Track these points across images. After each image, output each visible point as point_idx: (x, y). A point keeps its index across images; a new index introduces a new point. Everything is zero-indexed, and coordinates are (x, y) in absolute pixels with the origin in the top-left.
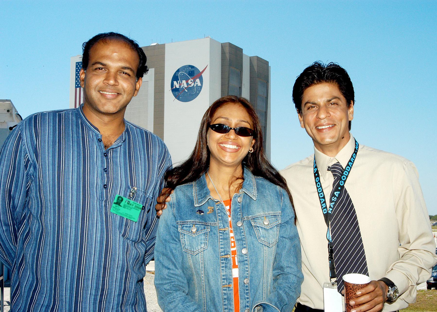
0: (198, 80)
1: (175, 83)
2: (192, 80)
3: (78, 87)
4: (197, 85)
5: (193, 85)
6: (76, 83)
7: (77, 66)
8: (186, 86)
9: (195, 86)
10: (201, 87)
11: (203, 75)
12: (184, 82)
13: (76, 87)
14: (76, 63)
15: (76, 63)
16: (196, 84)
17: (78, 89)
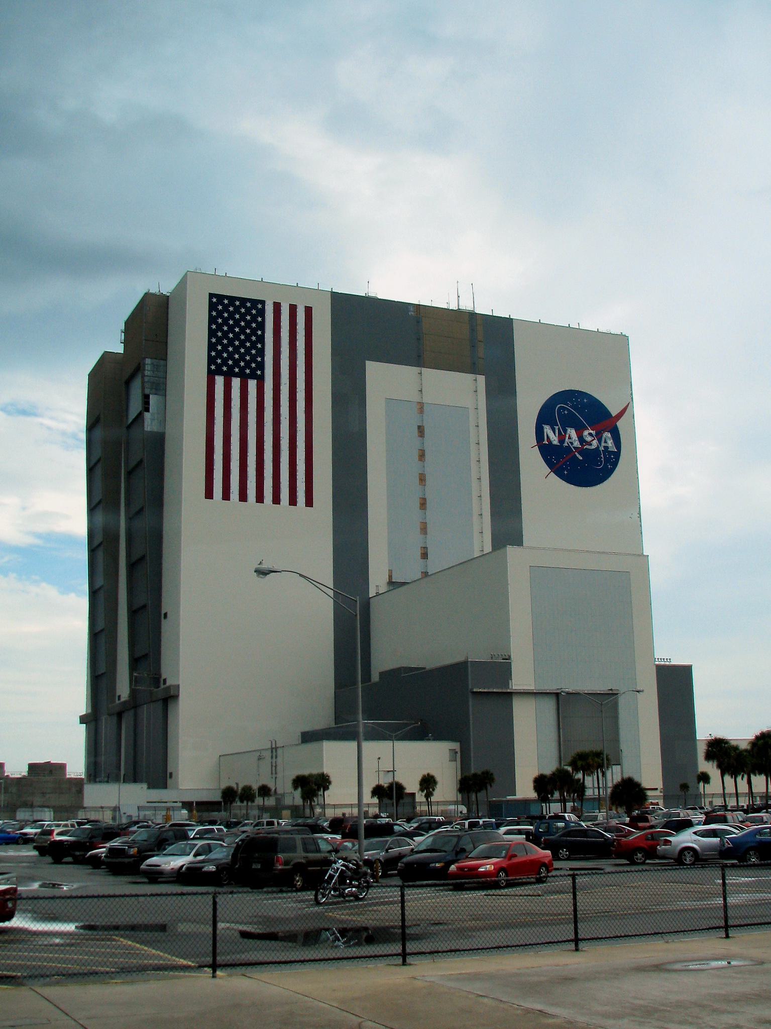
0: (607, 435)
1: (547, 430)
2: (593, 432)
3: (219, 372)
4: (606, 448)
5: (595, 443)
6: (211, 360)
7: (212, 307)
8: (577, 444)
9: (602, 448)
10: (617, 455)
11: (619, 424)
12: (572, 432)
13: (211, 375)
14: (211, 296)
15: (211, 296)
16: (603, 444)
17: (220, 380)
